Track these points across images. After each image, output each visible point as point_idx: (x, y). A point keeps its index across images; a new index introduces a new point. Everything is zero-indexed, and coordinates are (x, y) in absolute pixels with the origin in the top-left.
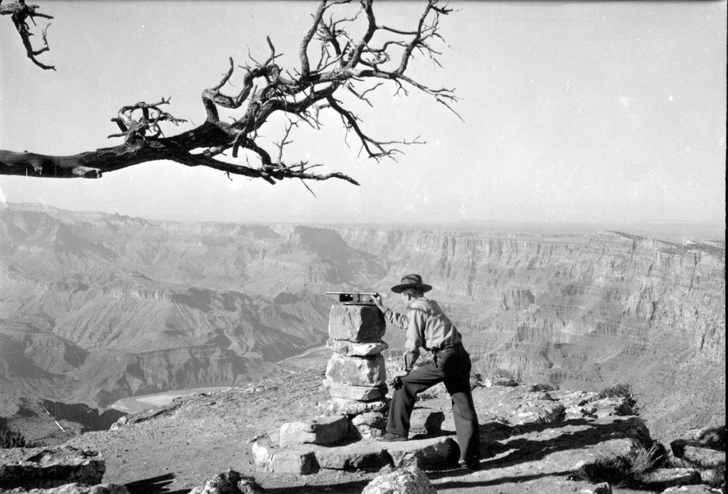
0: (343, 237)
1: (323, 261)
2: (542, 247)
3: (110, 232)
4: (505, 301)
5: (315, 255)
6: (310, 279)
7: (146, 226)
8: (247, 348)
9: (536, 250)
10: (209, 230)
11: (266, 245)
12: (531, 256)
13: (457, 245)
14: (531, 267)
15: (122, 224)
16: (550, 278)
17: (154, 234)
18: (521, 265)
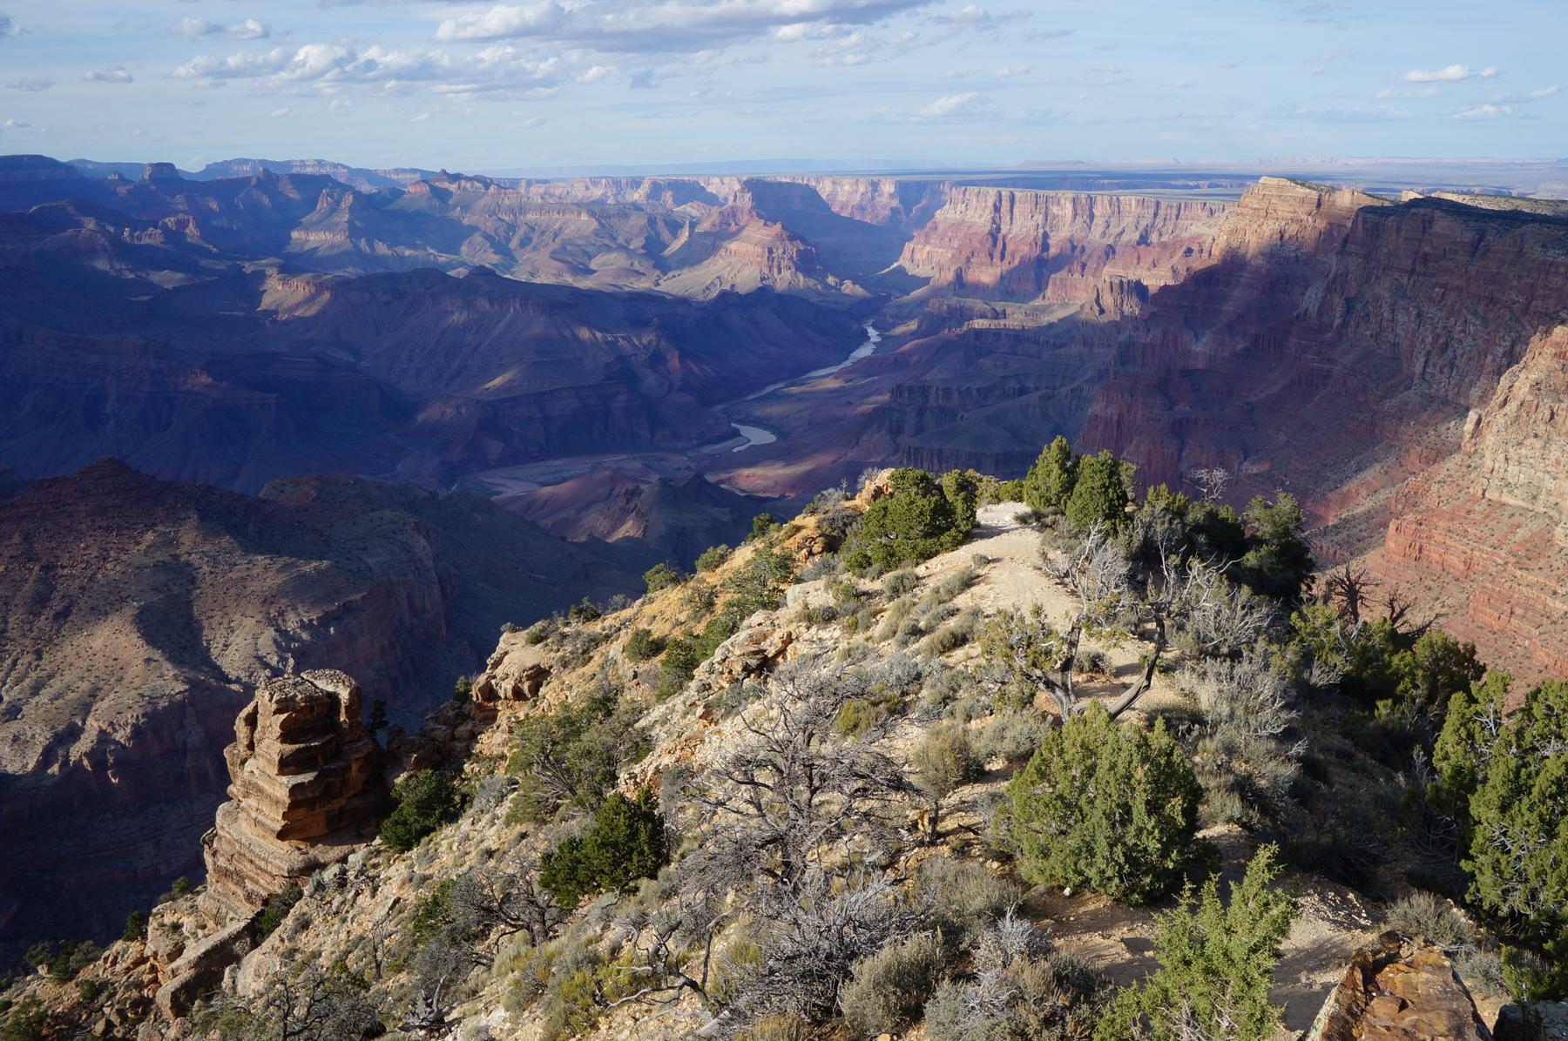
0: (824, 196)
1: (791, 239)
2: (1163, 205)
3: (436, 203)
4: (1097, 301)
5: (778, 227)
6: (771, 268)
7: (492, 189)
8: (671, 386)
9: (1152, 211)
10: (597, 193)
11: (695, 213)
12: (1144, 223)
13: (1017, 205)
14: (1144, 240)
15: (453, 187)
16: (1175, 259)
17: (507, 202)
18: (1125, 238)
